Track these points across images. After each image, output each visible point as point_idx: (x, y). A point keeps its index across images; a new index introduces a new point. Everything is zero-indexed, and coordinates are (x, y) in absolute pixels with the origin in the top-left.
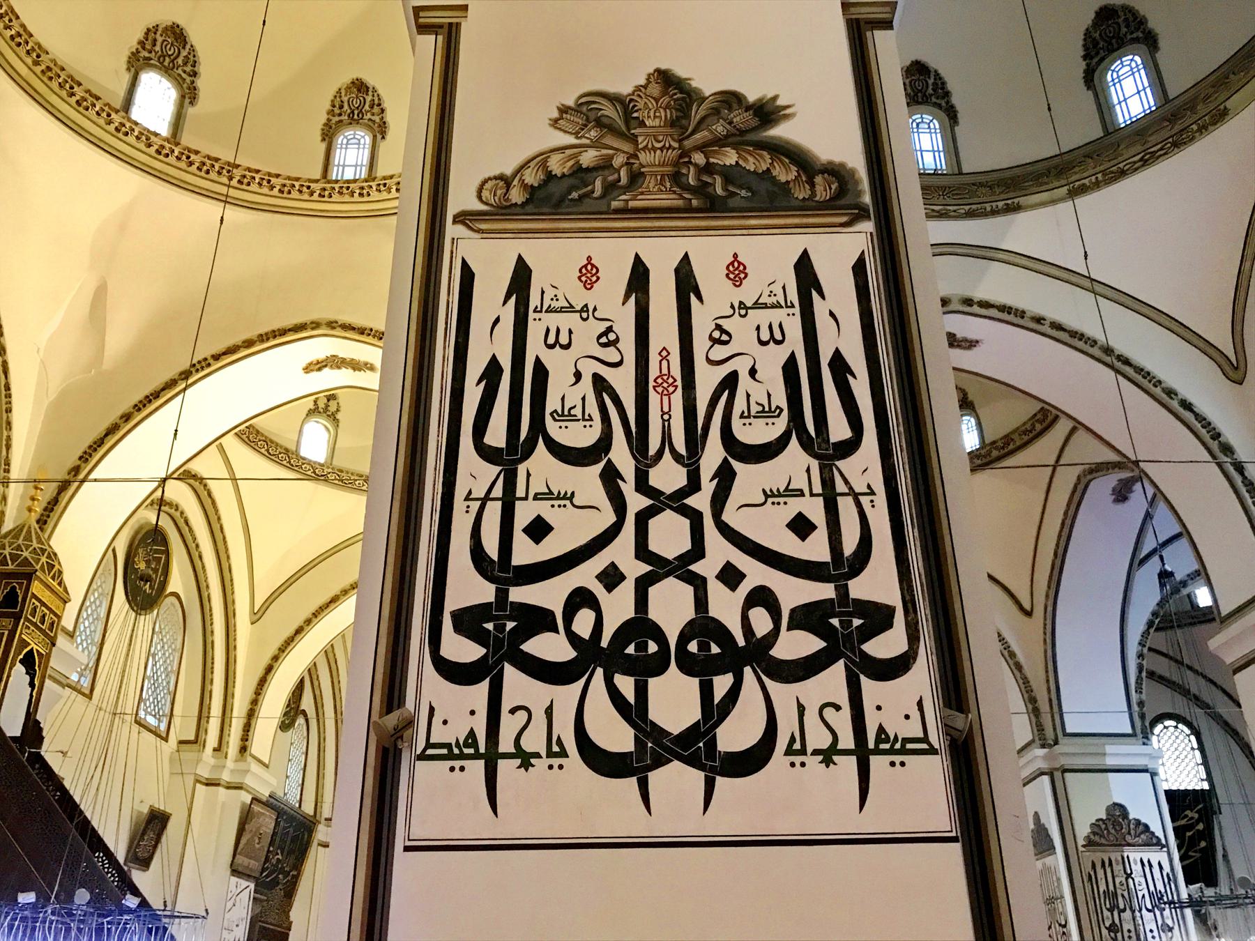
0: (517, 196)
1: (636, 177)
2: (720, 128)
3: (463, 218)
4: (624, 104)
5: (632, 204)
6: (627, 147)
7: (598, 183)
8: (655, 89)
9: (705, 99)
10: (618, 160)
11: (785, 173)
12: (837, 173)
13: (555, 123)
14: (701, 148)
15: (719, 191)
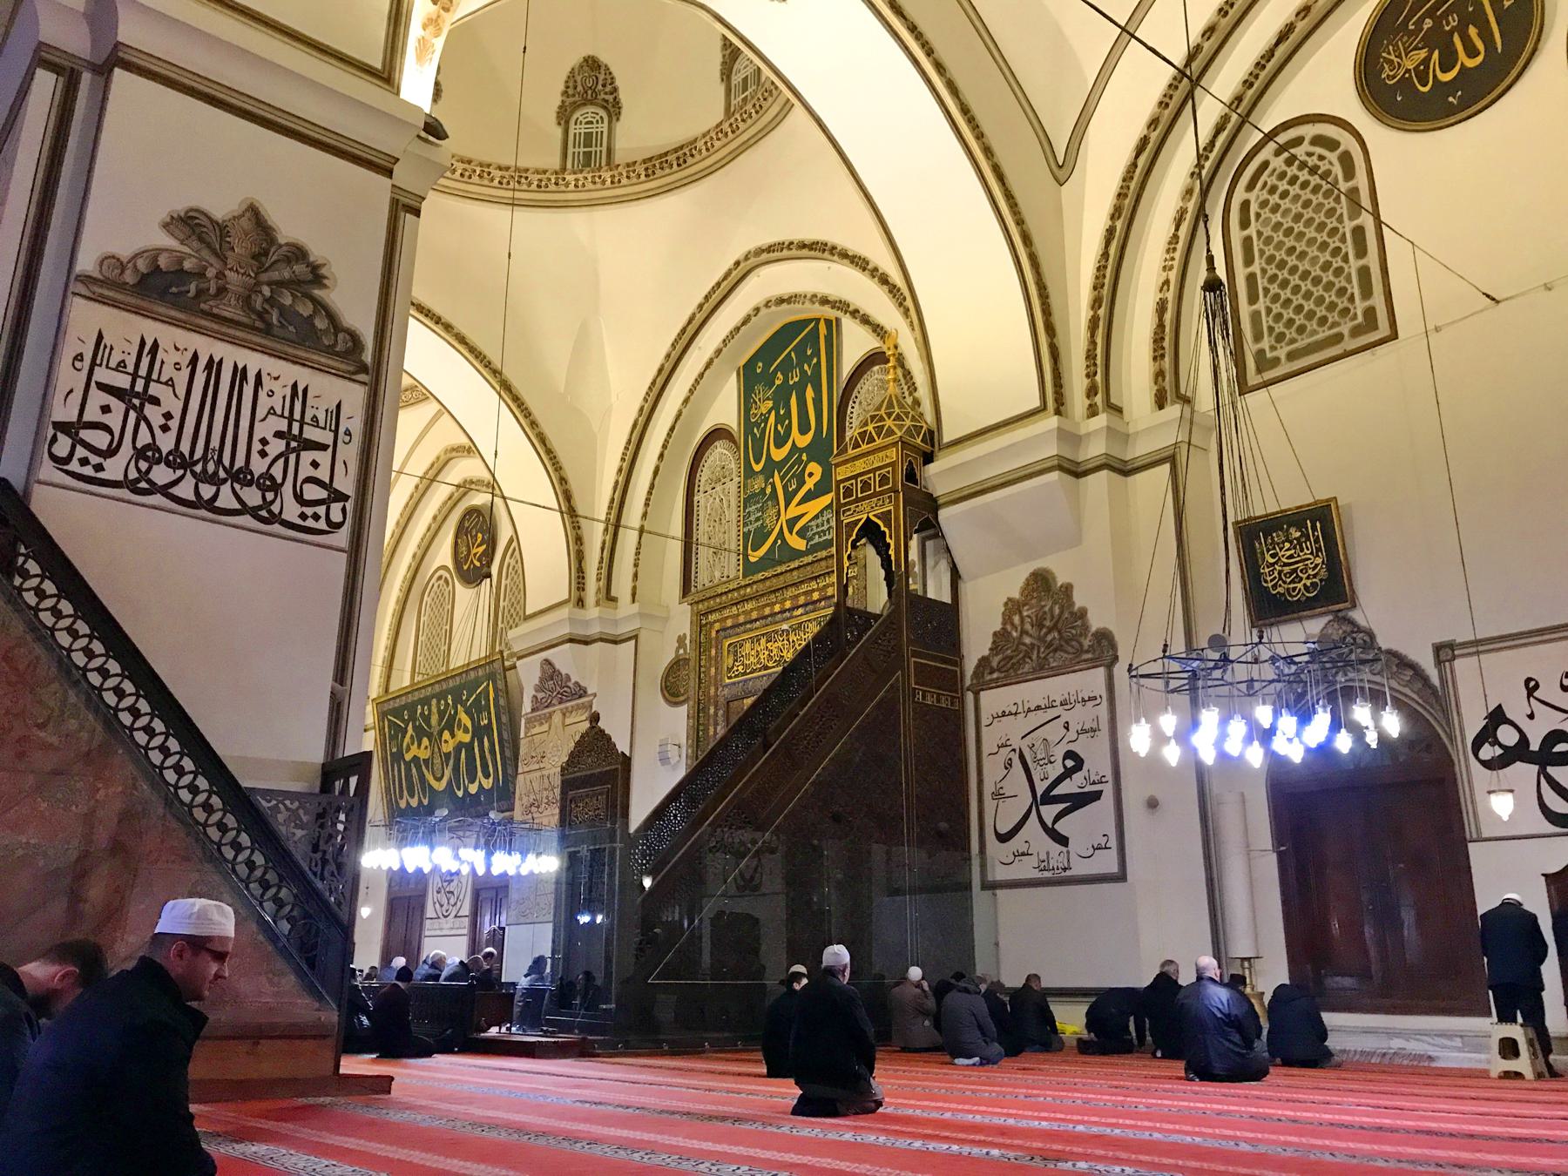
0: (129, 277)
1: (222, 290)
2: (287, 274)
3: (86, 279)
4: (222, 229)
5: (215, 311)
6: (217, 264)
7: (193, 287)
8: (245, 223)
9: (281, 246)
10: (211, 273)
11: (321, 323)
12: (355, 338)
13: (166, 226)
14: (269, 284)
15: (275, 321)
